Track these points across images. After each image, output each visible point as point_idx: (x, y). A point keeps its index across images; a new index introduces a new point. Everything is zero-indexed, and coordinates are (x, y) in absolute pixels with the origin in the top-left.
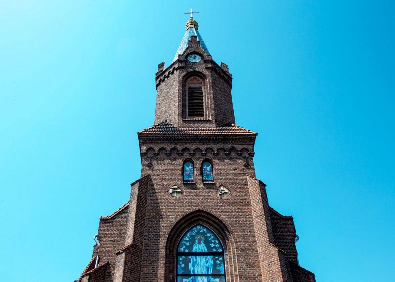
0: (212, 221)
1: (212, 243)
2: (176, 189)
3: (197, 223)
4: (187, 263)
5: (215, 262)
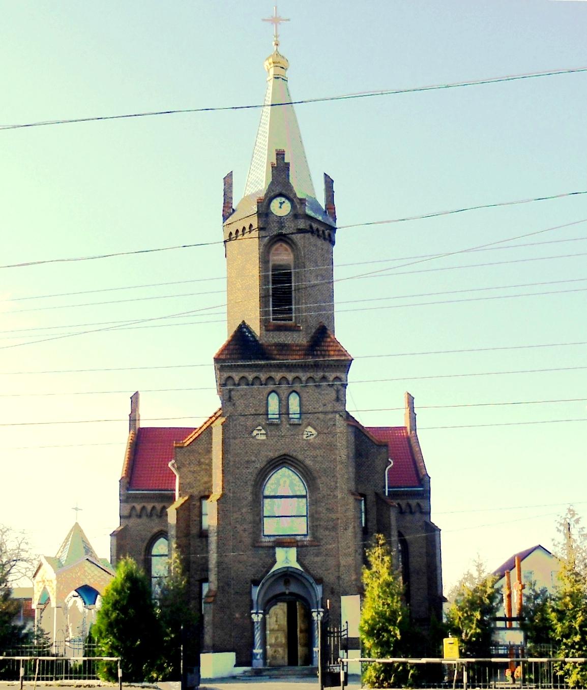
0: (297, 464)
1: (296, 485)
2: (260, 430)
3: (282, 466)
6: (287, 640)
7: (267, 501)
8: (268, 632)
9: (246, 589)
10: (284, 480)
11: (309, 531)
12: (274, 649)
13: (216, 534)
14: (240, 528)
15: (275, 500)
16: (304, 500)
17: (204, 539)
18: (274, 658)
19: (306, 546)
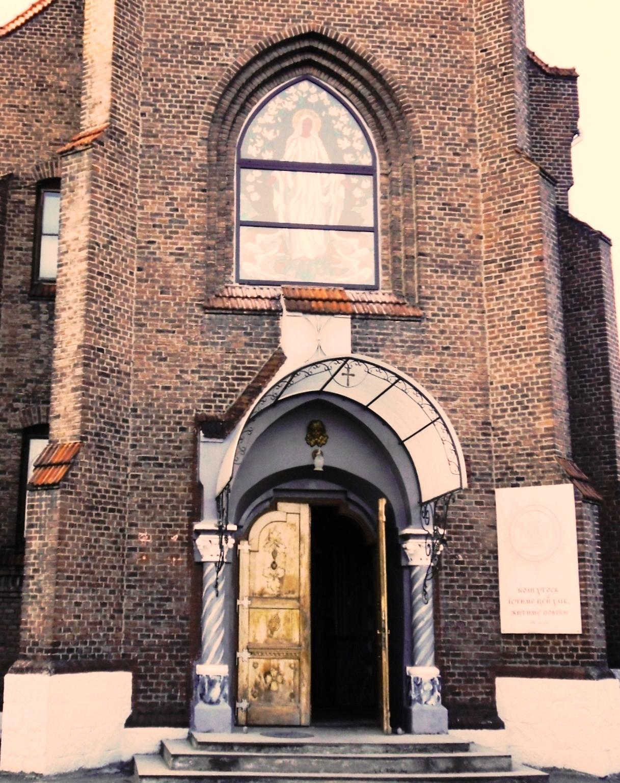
1: (342, 136)
3: (299, 72)
4: (267, 192)
5: (349, 193)
6: (308, 632)
7: (250, 176)
8: (243, 602)
9: (179, 448)
10: (304, 118)
11: (381, 278)
12: (262, 662)
13: (84, 253)
14: (164, 248)
15: (276, 174)
16: (367, 181)
17: (43, 306)
18: (264, 693)
19: (380, 317)
